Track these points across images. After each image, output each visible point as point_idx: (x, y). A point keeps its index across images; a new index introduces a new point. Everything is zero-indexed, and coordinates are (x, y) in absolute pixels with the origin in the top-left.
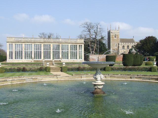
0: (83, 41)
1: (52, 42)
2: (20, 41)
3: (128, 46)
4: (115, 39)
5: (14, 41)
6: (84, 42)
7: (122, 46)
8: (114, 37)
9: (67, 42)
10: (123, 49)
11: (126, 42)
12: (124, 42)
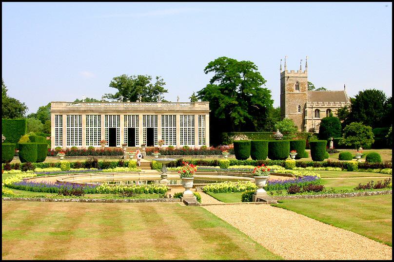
0: (206, 106)
2: (76, 109)
7: (314, 109)
8: (294, 87)
11: (323, 101)
12: (318, 101)
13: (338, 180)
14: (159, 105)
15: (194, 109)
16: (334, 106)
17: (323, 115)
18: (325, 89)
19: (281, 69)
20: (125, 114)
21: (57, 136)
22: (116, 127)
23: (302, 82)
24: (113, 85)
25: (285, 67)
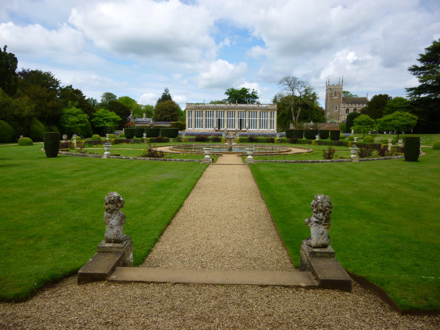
1: (237, 108)
3: (347, 110)
4: (336, 99)
5: (193, 107)
6: (278, 108)
7: (346, 109)
8: (333, 95)
9: (255, 108)
10: (346, 113)
11: (352, 103)
13: (138, 150)
14: (255, 105)
15: (267, 108)
16: (358, 107)
17: (351, 111)
18: (357, 96)
19: (326, 84)
20: (228, 110)
21: (189, 123)
22: (220, 118)
23: (339, 92)
24: (227, 93)
25: (329, 82)
